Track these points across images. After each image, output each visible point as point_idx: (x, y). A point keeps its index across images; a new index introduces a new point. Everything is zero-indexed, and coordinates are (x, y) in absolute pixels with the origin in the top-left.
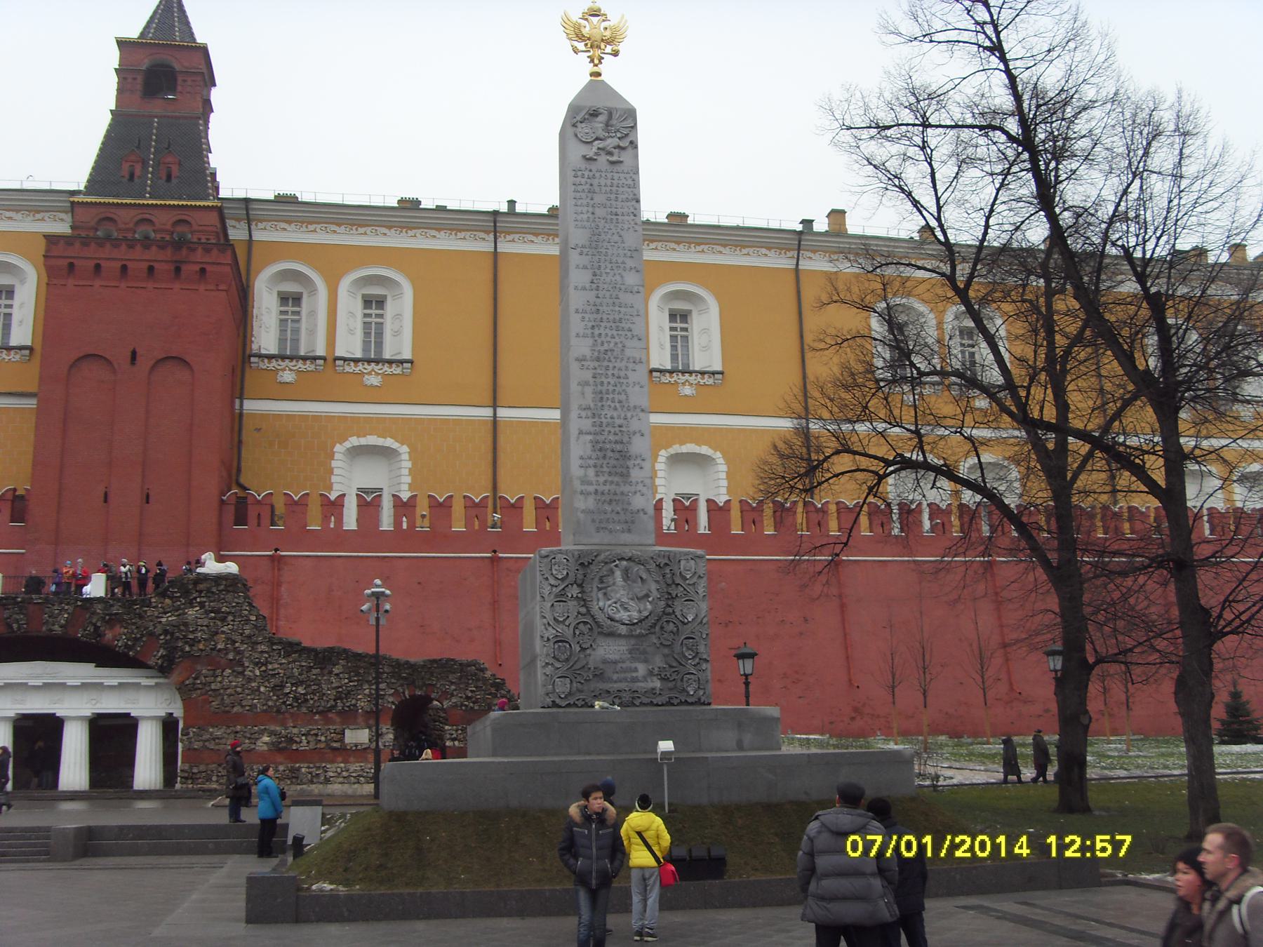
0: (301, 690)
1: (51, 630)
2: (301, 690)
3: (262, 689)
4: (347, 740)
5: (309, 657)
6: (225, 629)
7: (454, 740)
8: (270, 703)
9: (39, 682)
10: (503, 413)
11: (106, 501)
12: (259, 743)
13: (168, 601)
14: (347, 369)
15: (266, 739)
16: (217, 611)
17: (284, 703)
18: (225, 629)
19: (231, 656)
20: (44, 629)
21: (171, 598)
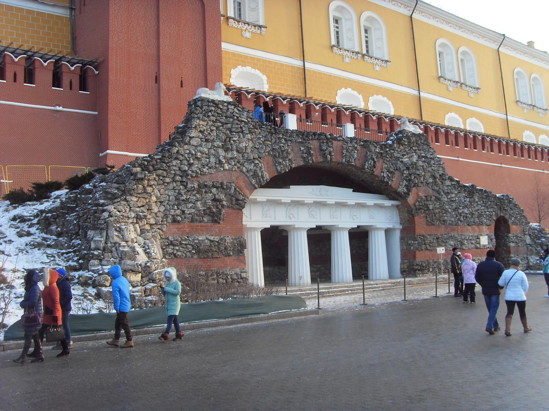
0: (466, 211)
1: (349, 161)
2: (466, 211)
3: (450, 210)
4: (482, 243)
5: (465, 191)
7: (513, 242)
8: (453, 220)
9: (332, 202)
10: (307, 65)
11: (156, 82)
12: (447, 244)
13: (401, 147)
14: (234, 25)
16: (426, 157)
17: (459, 219)
18: (430, 169)
20: (344, 160)
21: (402, 146)
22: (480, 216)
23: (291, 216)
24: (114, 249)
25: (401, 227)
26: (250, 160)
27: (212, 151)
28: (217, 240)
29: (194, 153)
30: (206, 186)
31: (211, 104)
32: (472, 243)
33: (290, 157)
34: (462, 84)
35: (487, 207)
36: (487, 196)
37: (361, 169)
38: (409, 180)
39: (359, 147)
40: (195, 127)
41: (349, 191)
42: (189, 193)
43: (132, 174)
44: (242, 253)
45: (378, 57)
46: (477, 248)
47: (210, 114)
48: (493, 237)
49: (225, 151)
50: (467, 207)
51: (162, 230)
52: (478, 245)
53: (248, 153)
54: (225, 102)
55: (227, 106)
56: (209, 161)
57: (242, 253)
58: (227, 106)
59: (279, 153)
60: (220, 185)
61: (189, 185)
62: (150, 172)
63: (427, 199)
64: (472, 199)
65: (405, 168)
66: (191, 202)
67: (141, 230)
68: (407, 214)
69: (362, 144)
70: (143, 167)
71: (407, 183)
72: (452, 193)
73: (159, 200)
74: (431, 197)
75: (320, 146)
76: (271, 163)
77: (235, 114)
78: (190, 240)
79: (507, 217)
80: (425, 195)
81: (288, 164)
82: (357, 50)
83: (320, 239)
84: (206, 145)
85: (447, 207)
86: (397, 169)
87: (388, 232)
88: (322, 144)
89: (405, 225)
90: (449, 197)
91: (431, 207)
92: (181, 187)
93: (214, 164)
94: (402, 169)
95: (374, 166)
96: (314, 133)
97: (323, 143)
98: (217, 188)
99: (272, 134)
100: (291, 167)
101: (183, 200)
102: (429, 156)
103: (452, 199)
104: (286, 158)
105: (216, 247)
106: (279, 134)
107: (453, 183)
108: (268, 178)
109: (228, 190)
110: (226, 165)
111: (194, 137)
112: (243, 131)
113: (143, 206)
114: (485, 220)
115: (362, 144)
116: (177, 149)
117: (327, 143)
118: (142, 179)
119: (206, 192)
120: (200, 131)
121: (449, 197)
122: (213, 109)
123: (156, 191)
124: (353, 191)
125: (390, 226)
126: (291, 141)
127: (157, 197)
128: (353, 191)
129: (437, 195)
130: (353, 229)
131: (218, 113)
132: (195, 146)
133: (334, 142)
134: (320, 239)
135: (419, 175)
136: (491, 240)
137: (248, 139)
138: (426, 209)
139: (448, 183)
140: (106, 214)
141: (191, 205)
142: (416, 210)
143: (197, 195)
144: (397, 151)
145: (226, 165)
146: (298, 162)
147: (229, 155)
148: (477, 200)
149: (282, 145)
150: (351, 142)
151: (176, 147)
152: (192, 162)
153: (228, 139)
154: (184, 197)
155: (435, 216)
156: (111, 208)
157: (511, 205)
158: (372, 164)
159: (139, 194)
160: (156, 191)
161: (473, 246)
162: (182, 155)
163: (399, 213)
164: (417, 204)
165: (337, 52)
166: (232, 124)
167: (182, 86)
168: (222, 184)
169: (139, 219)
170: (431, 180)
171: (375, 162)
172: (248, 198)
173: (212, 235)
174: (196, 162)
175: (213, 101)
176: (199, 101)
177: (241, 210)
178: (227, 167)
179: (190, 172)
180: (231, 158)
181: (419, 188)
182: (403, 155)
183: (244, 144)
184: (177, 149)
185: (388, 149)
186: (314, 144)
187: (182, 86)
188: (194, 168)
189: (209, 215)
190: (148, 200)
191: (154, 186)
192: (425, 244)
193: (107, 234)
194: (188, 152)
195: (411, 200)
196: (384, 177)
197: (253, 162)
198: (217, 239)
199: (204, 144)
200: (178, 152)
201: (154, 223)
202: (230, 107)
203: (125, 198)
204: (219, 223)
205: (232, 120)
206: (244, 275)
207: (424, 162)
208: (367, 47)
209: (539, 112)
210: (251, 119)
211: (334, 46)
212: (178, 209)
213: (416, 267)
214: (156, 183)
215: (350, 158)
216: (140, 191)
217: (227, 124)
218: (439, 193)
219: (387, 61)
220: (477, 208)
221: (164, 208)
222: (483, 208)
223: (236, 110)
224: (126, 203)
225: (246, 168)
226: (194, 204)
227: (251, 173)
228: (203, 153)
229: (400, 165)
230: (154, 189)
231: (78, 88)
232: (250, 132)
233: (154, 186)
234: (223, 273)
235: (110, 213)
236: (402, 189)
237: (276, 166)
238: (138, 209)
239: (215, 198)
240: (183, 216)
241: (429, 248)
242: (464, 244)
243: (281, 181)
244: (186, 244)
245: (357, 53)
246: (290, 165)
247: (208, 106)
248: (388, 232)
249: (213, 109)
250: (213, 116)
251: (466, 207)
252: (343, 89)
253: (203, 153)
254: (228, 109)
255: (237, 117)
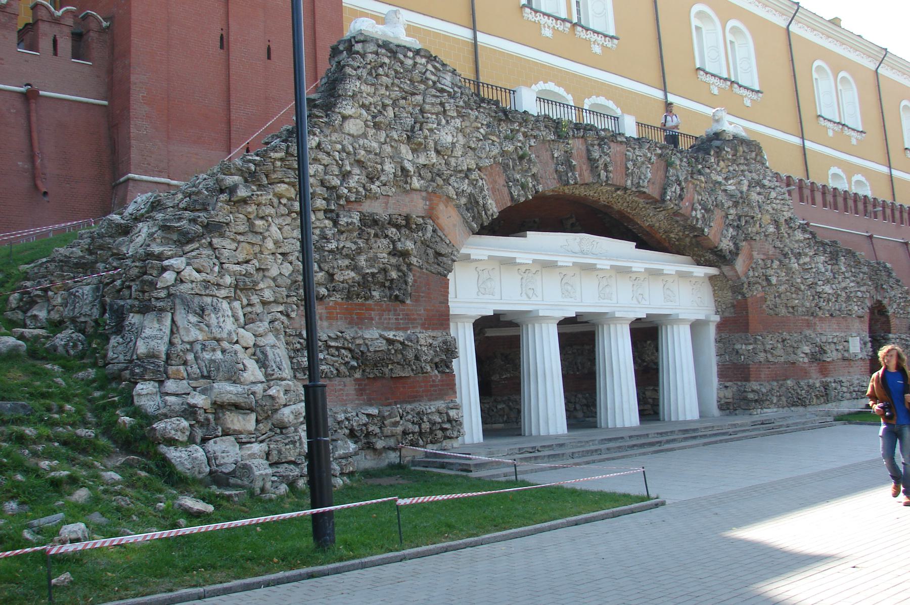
0: (827, 289)
2: (827, 289)
3: (803, 287)
4: (851, 352)
6: (769, 208)
8: (808, 305)
10: (481, 37)
11: (222, 47)
13: (722, 163)
15: (807, 349)
19: (778, 244)
20: (629, 182)
22: (848, 298)
23: (530, 293)
24: (190, 357)
25: (717, 318)
26: (460, 171)
27: (388, 149)
28: (401, 339)
29: (351, 149)
30: (375, 222)
31: (384, 51)
32: (837, 350)
33: (534, 170)
34: (732, 82)
35: (858, 283)
36: (858, 263)
37: (656, 201)
38: (738, 226)
39: (654, 158)
40: (353, 96)
41: (628, 247)
42: (343, 237)
43: (222, 191)
44: (448, 367)
45: (596, 29)
46: (844, 359)
47: (381, 71)
48: (868, 339)
49: (414, 151)
50: (828, 282)
51: (288, 316)
52: (846, 355)
53: (457, 158)
54: (409, 49)
55: (414, 58)
56: (383, 170)
57: (448, 367)
58: (414, 58)
59: (514, 160)
60: (404, 222)
61: (343, 220)
62: (260, 187)
63: (765, 265)
64: (836, 267)
65: (731, 203)
66: (347, 256)
67: (244, 315)
68: (730, 294)
69: (659, 151)
70: (247, 175)
71: (734, 233)
72: (806, 255)
73: (280, 251)
74: (772, 262)
75: (588, 151)
76: (501, 181)
77: (428, 75)
78: (345, 339)
79: (885, 302)
80: (762, 257)
81: (530, 185)
82: (564, 15)
83: (579, 341)
84: (375, 134)
85: (799, 280)
86: (717, 206)
87: (696, 327)
88: (591, 148)
89: (726, 314)
90: (801, 262)
91: (774, 280)
92: (327, 222)
93: (392, 176)
94: (726, 206)
95: (681, 197)
96: (576, 124)
97: (593, 145)
98: (398, 227)
99: (500, 120)
100: (537, 192)
101: (331, 251)
102: (766, 182)
103: (806, 267)
104: (526, 171)
105: (400, 356)
106: (512, 122)
107: (807, 236)
108: (495, 210)
109: (420, 234)
110: (415, 179)
111: (351, 117)
112: (445, 111)
113: (247, 262)
114: (856, 308)
115: (659, 151)
116: (317, 139)
117: (599, 145)
118: (245, 201)
119: (376, 235)
120: (363, 106)
121: (801, 262)
122: (387, 61)
123: (274, 229)
124: (637, 247)
125: (701, 317)
126: (535, 137)
127: (276, 243)
128: (637, 247)
129: (782, 258)
130: (638, 320)
131: (396, 72)
132: (353, 136)
133: (612, 145)
134: (579, 341)
135: (753, 218)
136: (865, 344)
137: (457, 128)
138: (764, 283)
139: (799, 235)
140: (169, 276)
141: (347, 262)
142: (749, 283)
143: (360, 241)
144: (715, 170)
145: (415, 179)
146: (549, 185)
147: (422, 160)
148: (844, 269)
149: (519, 144)
150: (640, 148)
151: (315, 134)
152: (348, 168)
153: (418, 125)
154: (333, 246)
155: (779, 296)
156: (178, 262)
157: (892, 281)
158: (678, 192)
159: (240, 234)
160: (274, 229)
161: (840, 356)
162: (328, 154)
163: (714, 291)
164: (751, 273)
165: (530, 16)
166: (424, 95)
167: (269, 58)
168: (407, 218)
169: (241, 290)
170: (771, 229)
171: (682, 189)
172: (458, 251)
173: (390, 330)
174: (356, 171)
175: (385, 45)
176: (357, 42)
177: (446, 276)
178: (416, 183)
179: (346, 191)
180: (425, 165)
181: (753, 243)
182: (726, 179)
183: (449, 139)
184: (317, 139)
185: (700, 166)
186: (576, 145)
187: (269, 58)
188: (352, 183)
189: (383, 285)
190: (257, 249)
191: (270, 219)
192: (765, 351)
193: (173, 321)
194: (339, 147)
195: (740, 264)
196: (697, 220)
197: (467, 177)
198: (400, 336)
199: (371, 132)
200: (319, 146)
201: (272, 299)
202: (419, 60)
203: (210, 244)
204: (403, 302)
205: (422, 87)
206: (452, 413)
207: (759, 194)
208: (578, 12)
209: (849, 136)
210: (460, 88)
211: (524, 6)
212: (321, 269)
213: (751, 396)
214: (273, 211)
215: (640, 178)
216: (242, 228)
217: (413, 94)
218: (786, 255)
219: (612, 37)
220: (843, 285)
221: (291, 268)
222: (852, 284)
223: (430, 67)
224: (211, 252)
225: (453, 187)
226: (353, 259)
227: (463, 200)
228: (370, 152)
229: (721, 197)
230: (269, 226)
231: (70, 54)
232: (461, 115)
233: (270, 219)
234: (413, 410)
235: (178, 273)
236: (726, 244)
237: (509, 187)
238: (237, 268)
239: (395, 248)
240: (330, 286)
241: (771, 359)
242: (825, 352)
243: (512, 222)
244: (337, 348)
245: (564, 20)
246: (534, 186)
247: (377, 53)
248: (696, 327)
249: (387, 61)
250: (387, 76)
251: (827, 281)
252: (541, 83)
253: (370, 152)
254: (415, 64)
255: (434, 83)
